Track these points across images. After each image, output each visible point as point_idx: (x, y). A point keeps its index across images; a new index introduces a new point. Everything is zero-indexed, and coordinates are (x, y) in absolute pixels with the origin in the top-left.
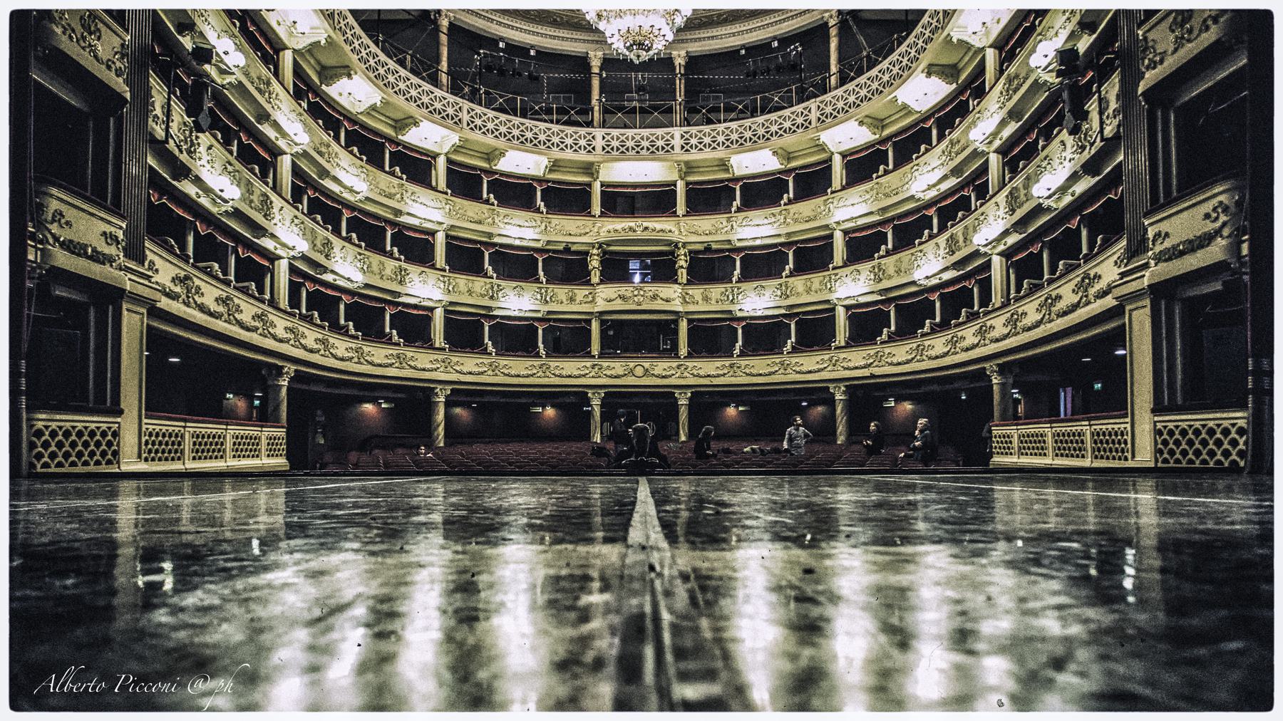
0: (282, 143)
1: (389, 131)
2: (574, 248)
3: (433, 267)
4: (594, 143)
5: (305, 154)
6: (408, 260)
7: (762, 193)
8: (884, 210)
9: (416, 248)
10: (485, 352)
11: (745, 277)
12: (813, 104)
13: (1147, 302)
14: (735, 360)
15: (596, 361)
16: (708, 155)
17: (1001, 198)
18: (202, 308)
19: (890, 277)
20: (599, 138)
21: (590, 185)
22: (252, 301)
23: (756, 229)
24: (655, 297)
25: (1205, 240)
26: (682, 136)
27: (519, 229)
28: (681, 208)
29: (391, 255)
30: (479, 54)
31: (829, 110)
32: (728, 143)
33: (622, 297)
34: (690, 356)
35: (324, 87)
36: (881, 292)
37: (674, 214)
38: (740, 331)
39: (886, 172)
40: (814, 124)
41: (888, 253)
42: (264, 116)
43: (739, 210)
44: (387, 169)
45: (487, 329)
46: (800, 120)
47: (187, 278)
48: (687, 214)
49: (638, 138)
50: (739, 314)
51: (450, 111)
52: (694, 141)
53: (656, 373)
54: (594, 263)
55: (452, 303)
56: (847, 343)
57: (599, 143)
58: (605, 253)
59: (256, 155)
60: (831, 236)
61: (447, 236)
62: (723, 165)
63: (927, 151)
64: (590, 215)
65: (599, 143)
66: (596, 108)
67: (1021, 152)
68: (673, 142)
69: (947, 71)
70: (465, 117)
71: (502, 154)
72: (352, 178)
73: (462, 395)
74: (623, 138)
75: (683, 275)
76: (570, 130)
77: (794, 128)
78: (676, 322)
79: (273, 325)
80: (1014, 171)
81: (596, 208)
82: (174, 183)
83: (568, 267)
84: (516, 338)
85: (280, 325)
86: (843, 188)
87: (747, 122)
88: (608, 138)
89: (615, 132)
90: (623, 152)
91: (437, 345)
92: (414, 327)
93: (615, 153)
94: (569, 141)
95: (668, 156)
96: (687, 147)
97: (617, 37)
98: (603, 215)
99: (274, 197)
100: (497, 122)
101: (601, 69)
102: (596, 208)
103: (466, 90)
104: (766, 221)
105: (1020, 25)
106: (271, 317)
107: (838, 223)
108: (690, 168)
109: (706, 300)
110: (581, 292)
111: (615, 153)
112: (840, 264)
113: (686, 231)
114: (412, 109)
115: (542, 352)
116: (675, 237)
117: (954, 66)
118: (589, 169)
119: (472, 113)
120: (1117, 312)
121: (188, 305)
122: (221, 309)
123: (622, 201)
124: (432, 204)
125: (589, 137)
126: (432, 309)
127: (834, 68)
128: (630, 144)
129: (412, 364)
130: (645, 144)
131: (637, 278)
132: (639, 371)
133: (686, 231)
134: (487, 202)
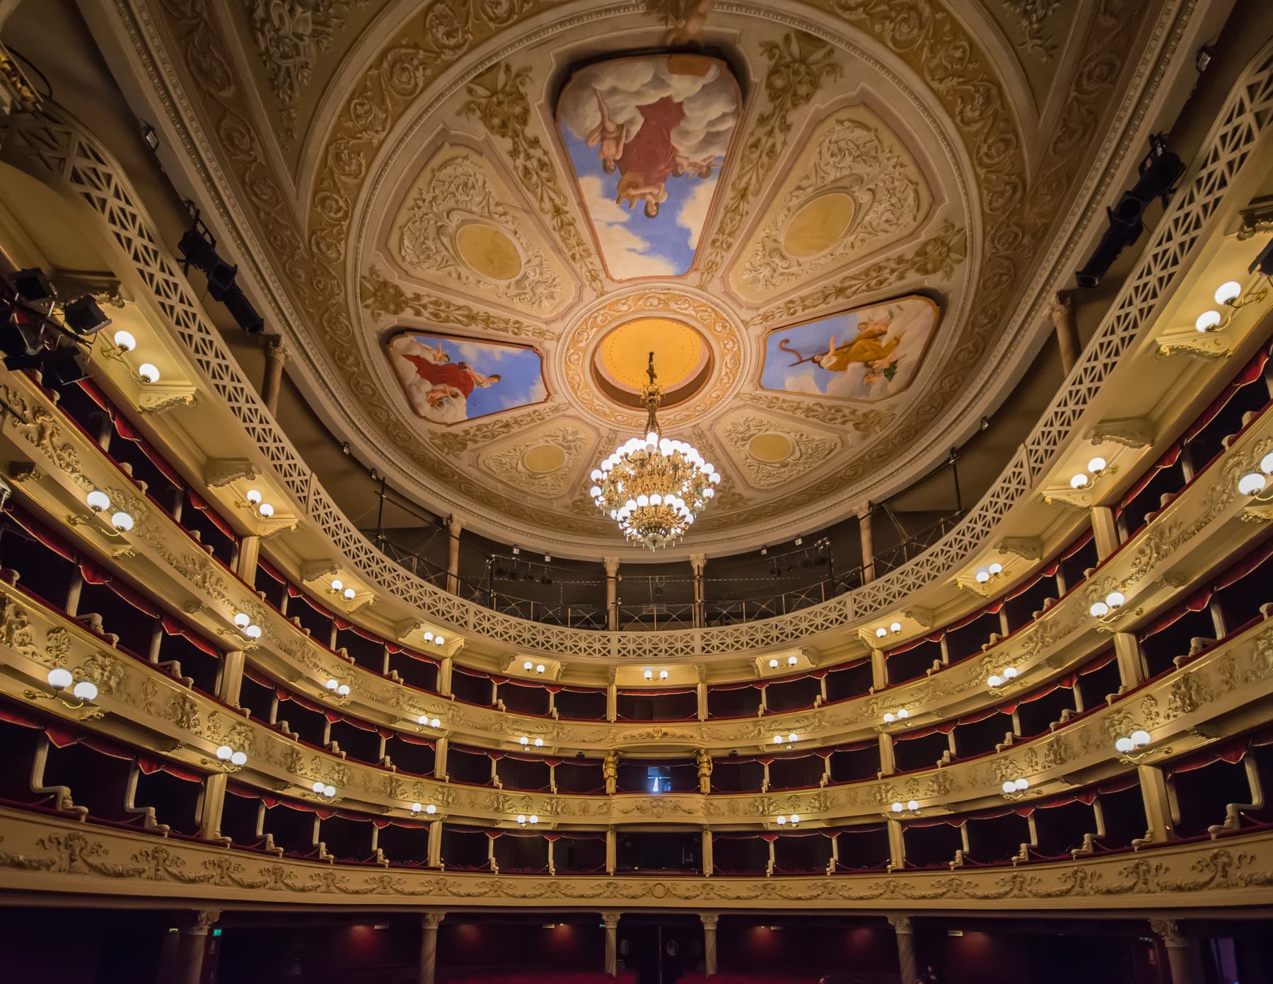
4: (609, 646)
11: (776, 786)
14: (768, 880)
15: (611, 879)
21: (605, 690)
27: (529, 737)
30: (490, 558)
32: (752, 643)
36: (948, 806)
39: (942, 668)
40: (850, 617)
49: (655, 640)
56: (906, 864)
57: (614, 646)
65: (614, 646)
74: (640, 641)
76: (584, 633)
88: (623, 640)
94: (583, 645)
95: (687, 658)
100: (506, 624)
101: (618, 573)
111: (631, 656)
113: (710, 737)
115: (552, 869)
125: (605, 640)
127: (867, 559)
130: (664, 646)
131: (656, 788)
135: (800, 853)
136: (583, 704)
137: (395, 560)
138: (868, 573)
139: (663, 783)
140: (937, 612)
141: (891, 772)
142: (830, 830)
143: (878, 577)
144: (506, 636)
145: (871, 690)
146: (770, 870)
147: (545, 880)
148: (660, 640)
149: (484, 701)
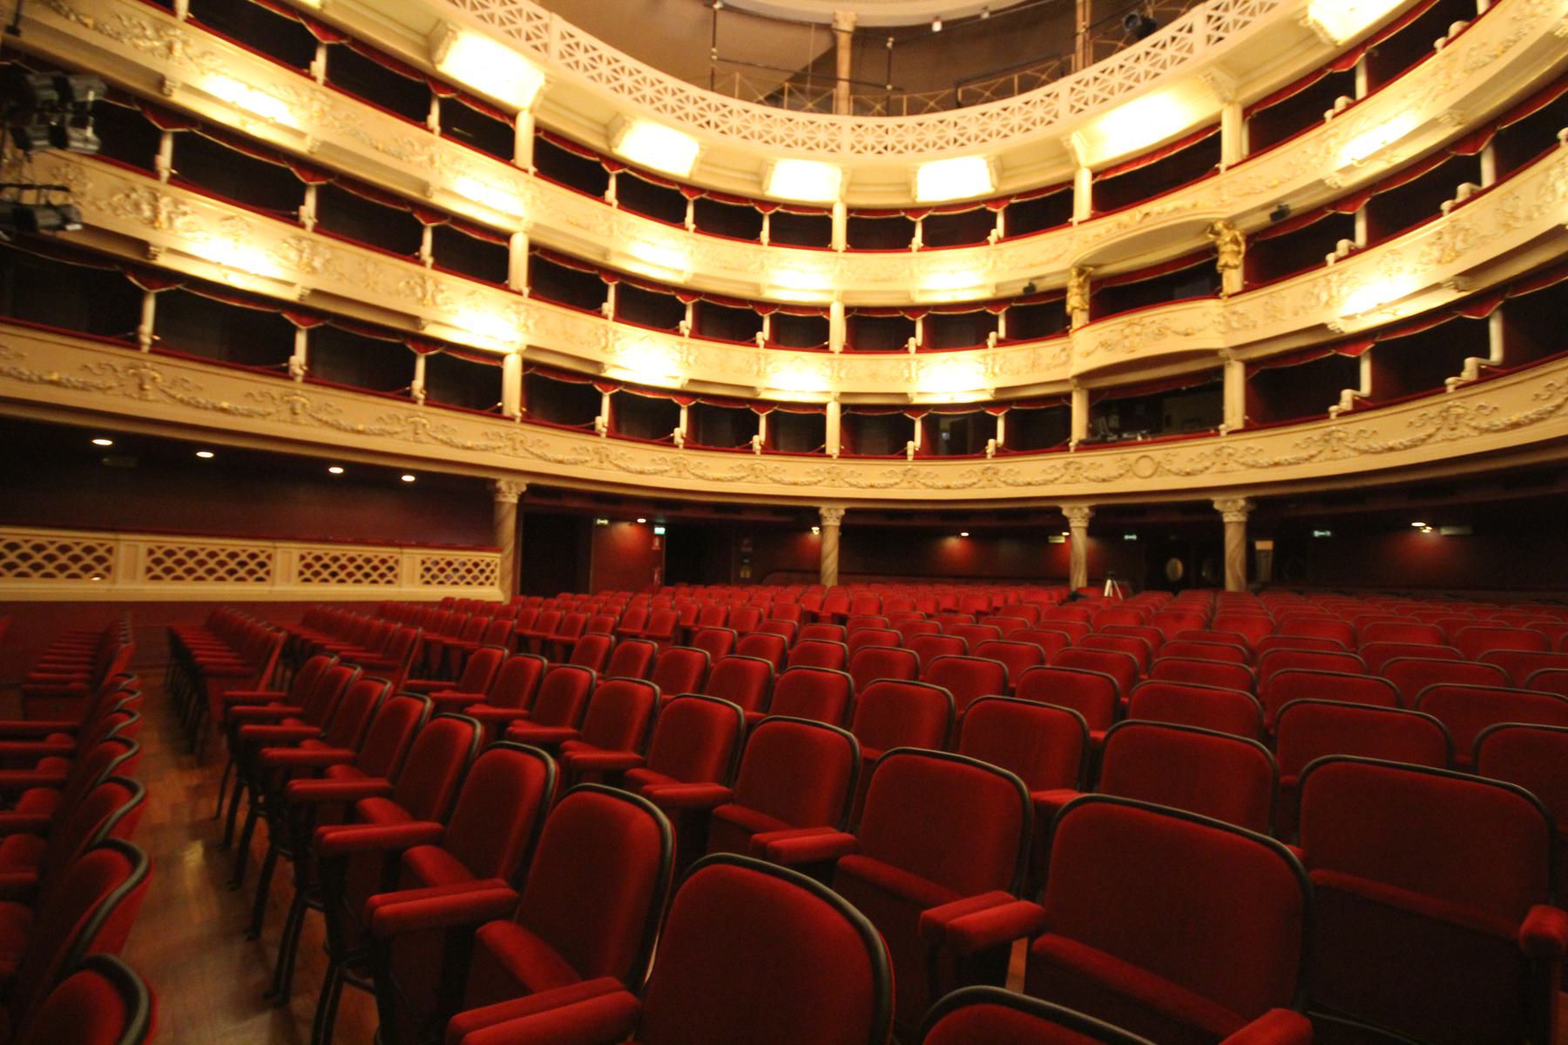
24: (1161, 333)
33: (1104, 345)
53: (1174, 468)
75: (1233, 279)
83: (1036, 315)
84: (959, 432)
132: (1146, 467)
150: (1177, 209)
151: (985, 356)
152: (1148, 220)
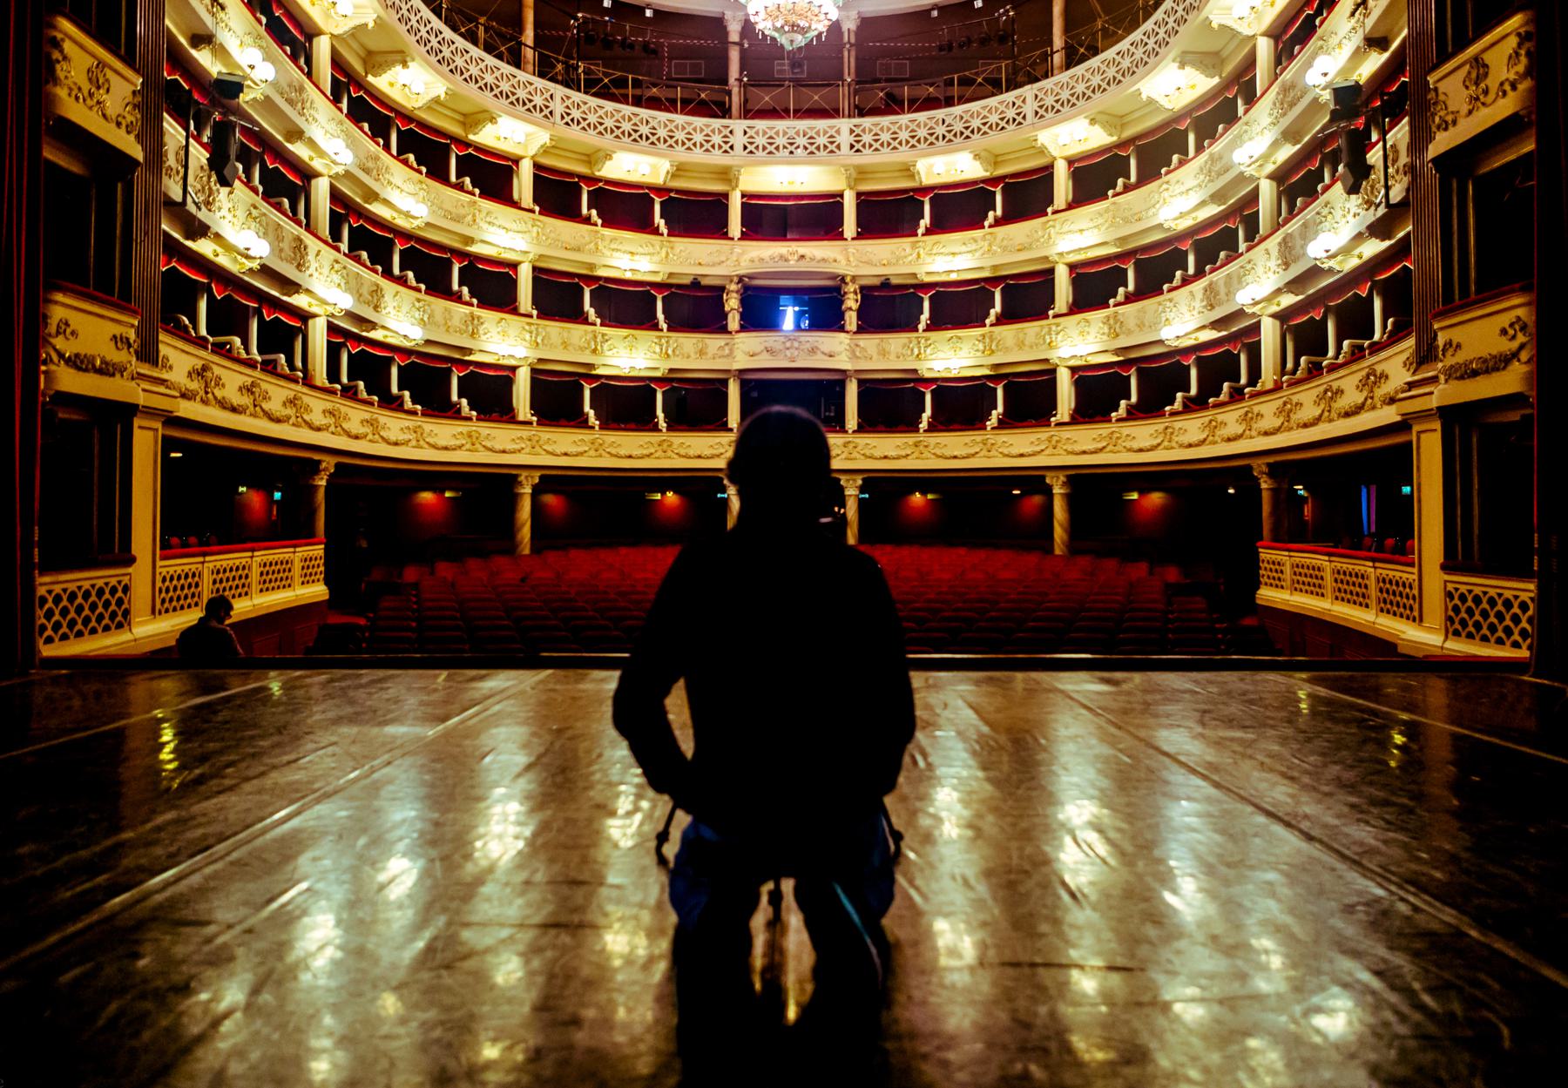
0: (317, 164)
1: (455, 129)
2: (705, 282)
3: (514, 311)
4: (732, 140)
5: (348, 175)
6: (481, 305)
7: (959, 208)
8: (1123, 240)
9: (492, 286)
10: (583, 423)
11: (935, 325)
12: (1028, 91)
13: (1437, 425)
14: (921, 436)
16: (886, 157)
17: (1273, 243)
18: (224, 405)
19: (1129, 332)
20: (739, 133)
21: (726, 196)
22: (282, 383)
23: (949, 258)
24: (813, 351)
25: (1499, 363)
26: (852, 131)
27: (632, 257)
28: (850, 226)
29: (458, 298)
30: (576, 19)
31: (1049, 101)
32: (913, 142)
34: (861, 429)
35: (370, 78)
37: (840, 236)
38: (928, 398)
39: (1128, 188)
41: (1130, 299)
42: (296, 134)
43: (928, 232)
44: (453, 178)
45: (587, 394)
46: (1011, 113)
47: (205, 368)
48: (860, 236)
49: (791, 133)
50: (928, 375)
51: (538, 101)
52: (867, 138)
54: (732, 303)
55: (540, 360)
58: (746, 288)
59: (284, 184)
60: (1051, 271)
61: (535, 269)
62: (908, 170)
63: (1181, 163)
64: (725, 236)
65: (739, 140)
66: (735, 91)
67: (1298, 185)
68: (838, 139)
69: (1206, 60)
70: (558, 107)
71: (608, 157)
72: (408, 200)
73: (553, 481)
74: (771, 133)
75: (851, 320)
77: (1003, 124)
78: (841, 384)
79: (308, 409)
80: (1292, 214)
81: (735, 225)
82: (189, 243)
83: (695, 307)
84: (626, 404)
85: (317, 406)
86: (1070, 207)
87: (940, 113)
89: (761, 124)
90: (771, 150)
91: (521, 418)
92: (489, 393)
93: (760, 153)
94: (698, 138)
95: (832, 157)
96: (858, 146)
97: (762, 15)
98: (745, 237)
99: (309, 239)
102: (735, 225)
103: (560, 67)
104: (964, 248)
105: (1301, 11)
106: (306, 399)
107: (1061, 254)
108: (862, 173)
109: (887, 354)
110: (714, 342)
111: (760, 153)
112: (1064, 310)
113: (856, 259)
114: (486, 100)
116: (841, 269)
117: (1217, 54)
118: (726, 174)
119: (568, 103)
120: (1403, 426)
121: (204, 402)
122: (245, 400)
123: (771, 218)
124: (513, 226)
126: (514, 369)
127: (1058, 41)
128: (781, 141)
129: (489, 444)
130: (802, 141)
131: (788, 322)
133: (856, 259)
134: (587, 221)
135: (961, 405)
136: (697, 214)
137: (455, 29)
138: (1058, 59)
139: (799, 317)
140: (1126, 120)
141: (1064, 310)
142: (996, 378)
143: (1068, 68)
144: (601, 128)
145: (1049, 210)
146: (924, 425)
147: (652, 437)
148: (798, 133)
149: (570, 212)
150: (823, 260)
151: (660, 338)
152: (802, 263)
